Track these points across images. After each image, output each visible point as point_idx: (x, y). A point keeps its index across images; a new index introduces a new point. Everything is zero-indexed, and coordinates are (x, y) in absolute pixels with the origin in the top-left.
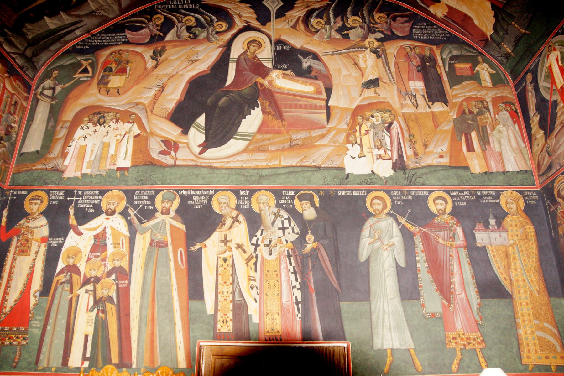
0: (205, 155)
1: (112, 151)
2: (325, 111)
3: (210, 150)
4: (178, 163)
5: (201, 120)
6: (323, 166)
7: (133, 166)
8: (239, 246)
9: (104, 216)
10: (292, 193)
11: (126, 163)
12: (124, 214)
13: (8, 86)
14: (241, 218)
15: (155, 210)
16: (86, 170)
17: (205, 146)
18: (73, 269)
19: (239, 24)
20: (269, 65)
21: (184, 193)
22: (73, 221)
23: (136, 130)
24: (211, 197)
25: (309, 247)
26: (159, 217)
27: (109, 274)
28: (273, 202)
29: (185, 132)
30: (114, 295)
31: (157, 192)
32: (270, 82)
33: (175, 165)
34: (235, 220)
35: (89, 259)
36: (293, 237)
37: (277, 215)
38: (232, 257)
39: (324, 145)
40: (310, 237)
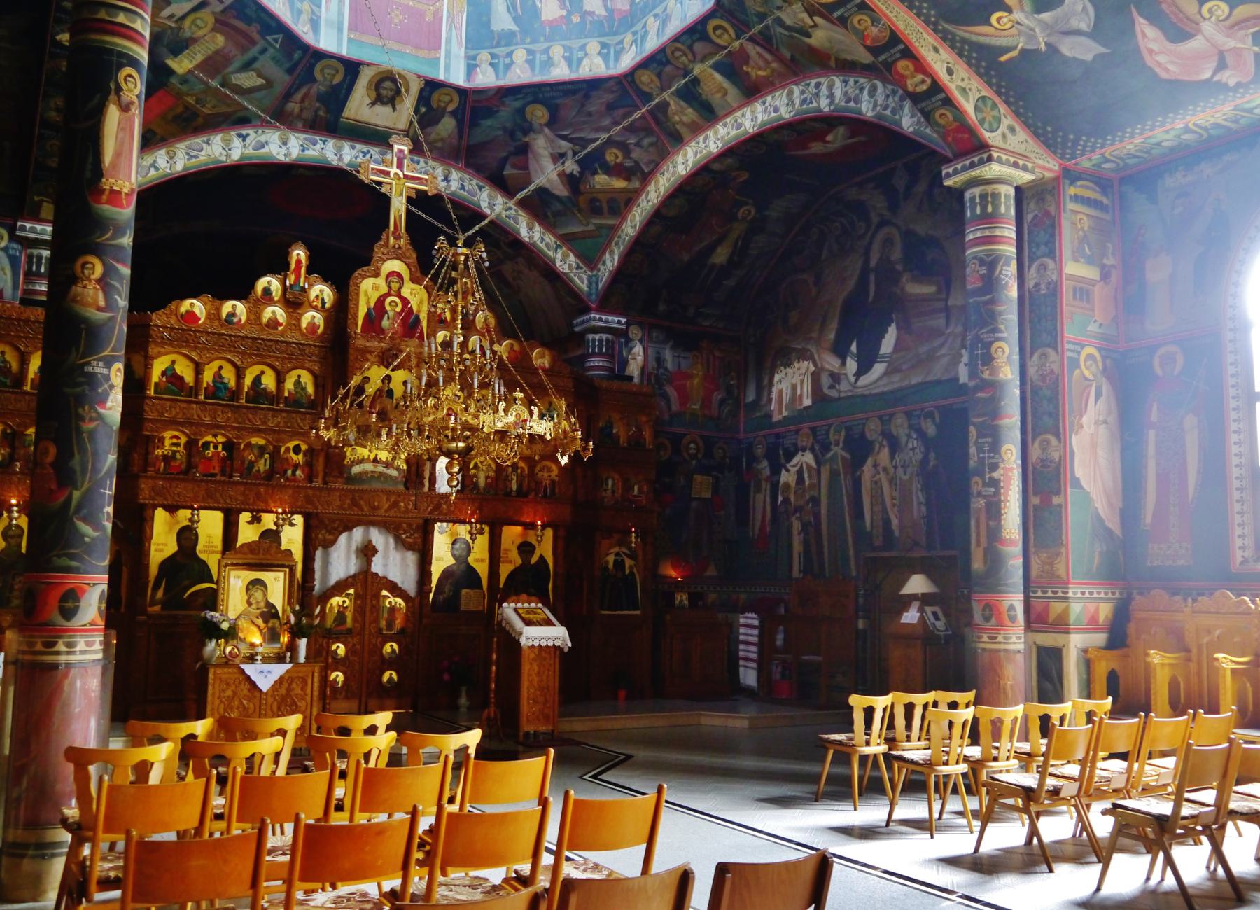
0: (860, 383)
1: (799, 393)
2: (944, 314)
3: (862, 378)
4: (843, 395)
5: (854, 348)
6: (944, 378)
7: (814, 402)
8: (885, 469)
9: (800, 453)
10: (918, 413)
11: (807, 402)
12: (813, 450)
13: (717, 354)
14: (885, 443)
15: (830, 444)
16: (785, 413)
17: (859, 374)
18: (786, 500)
19: (875, 220)
20: (899, 267)
21: (848, 424)
22: (783, 461)
23: (812, 368)
24: (864, 424)
25: (932, 464)
26: (835, 449)
27: (808, 503)
28: (906, 425)
29: (844, 364)
30: (812, 519)
31: (830, 426)
32: (903, 289)
33: (840, 399)
34: (881, 446)
35: (796, 492)
36: (919, 456)
37: (909, 436)
38: (880, 479)
39: (944, 355)
40: (932, 455)
